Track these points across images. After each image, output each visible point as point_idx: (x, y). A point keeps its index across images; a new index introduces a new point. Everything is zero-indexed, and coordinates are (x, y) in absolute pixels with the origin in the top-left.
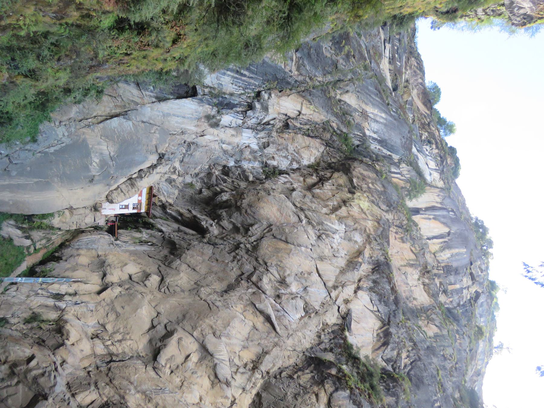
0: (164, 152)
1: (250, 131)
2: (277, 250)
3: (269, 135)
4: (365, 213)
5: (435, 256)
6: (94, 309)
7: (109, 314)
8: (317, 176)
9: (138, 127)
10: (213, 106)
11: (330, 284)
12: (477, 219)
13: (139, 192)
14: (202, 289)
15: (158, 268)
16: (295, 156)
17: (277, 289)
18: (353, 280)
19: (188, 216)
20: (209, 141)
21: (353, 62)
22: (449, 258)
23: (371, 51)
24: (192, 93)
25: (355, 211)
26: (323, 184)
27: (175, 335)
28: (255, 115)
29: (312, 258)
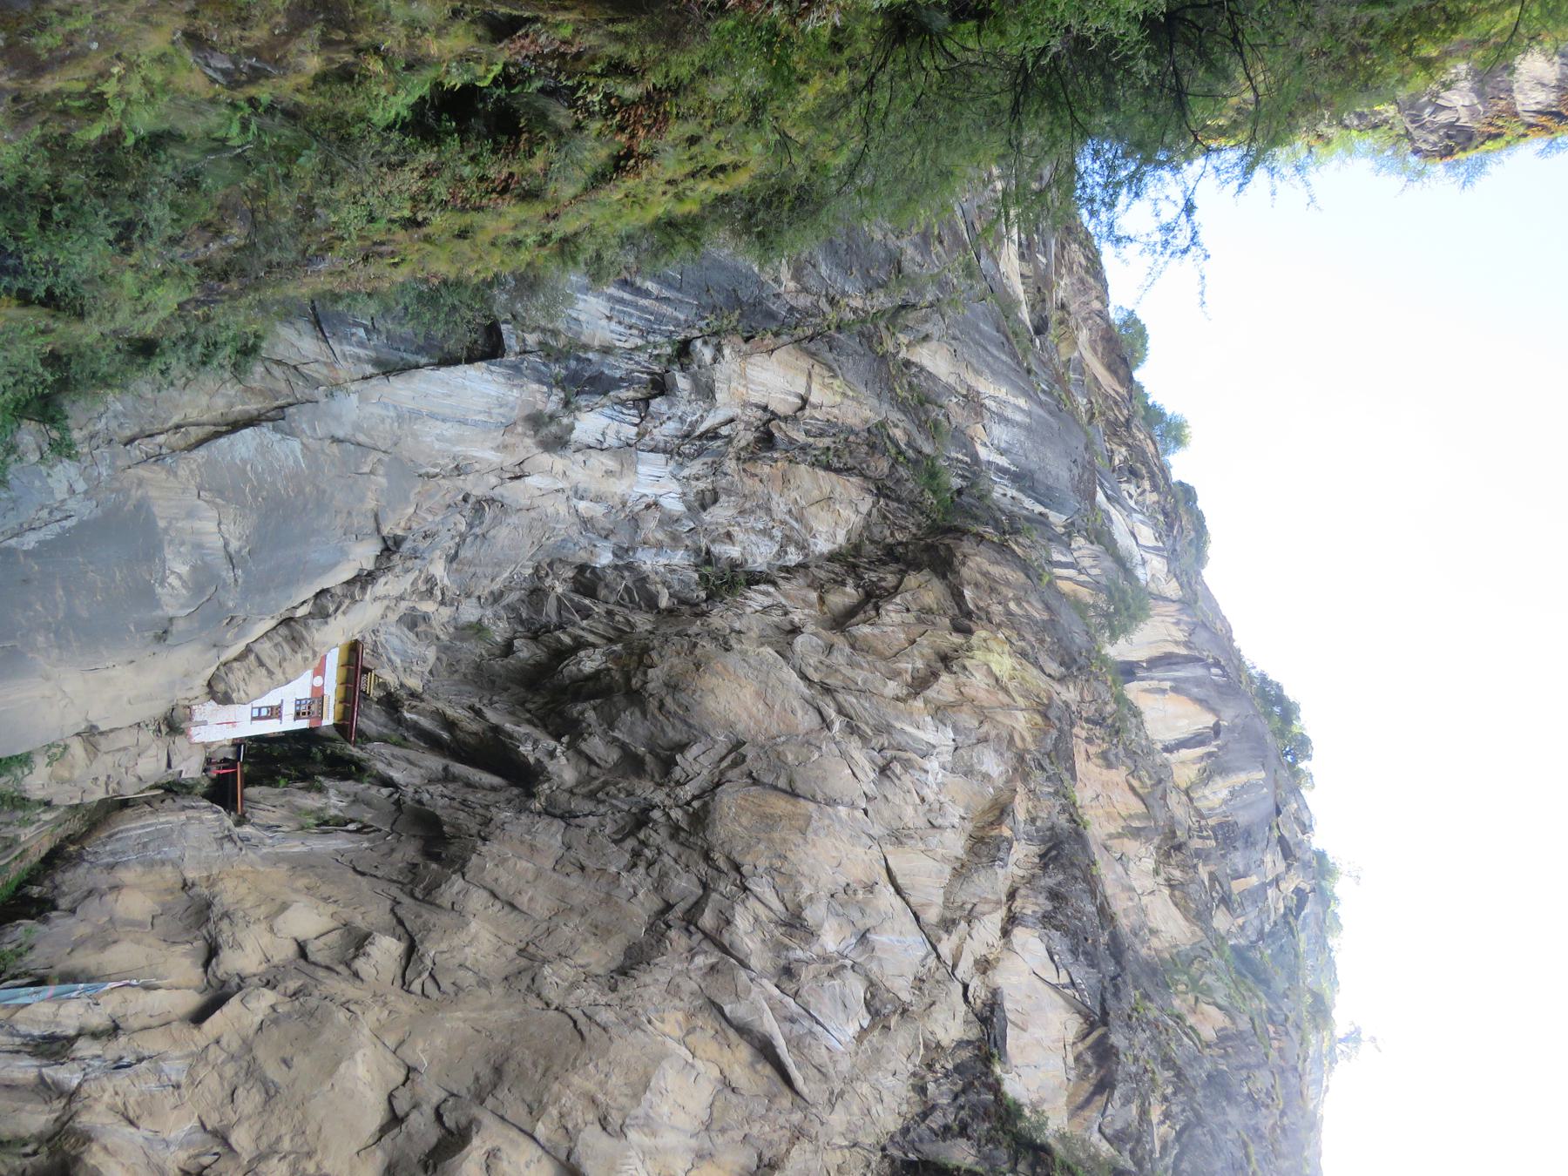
0: (400, 532)
1: (661, 458)
2: (768, 822)
3: (716, 469)
4: (1006, 691)
5: (1191, 800)
6: (183, 1080)
7: (240, 1091)
8: (857, 586)
9: (322, 458)
10: (550, 386)
11: (932, 915)
12: (1263, 678)
13: (317, 662)
14: (547, 970)
15: (392, 910)
16: (792, 528)
17: (779, 948)
18: (994, 898)
19: (475, 727)
20: (538, 493)
21: (938, 257)
22: (1225, 802)
23: (977, 225)
24: (488, 348)
25: (978, 684)
26: (877, 609)
27: (476, 1141)
29: (870, 836)
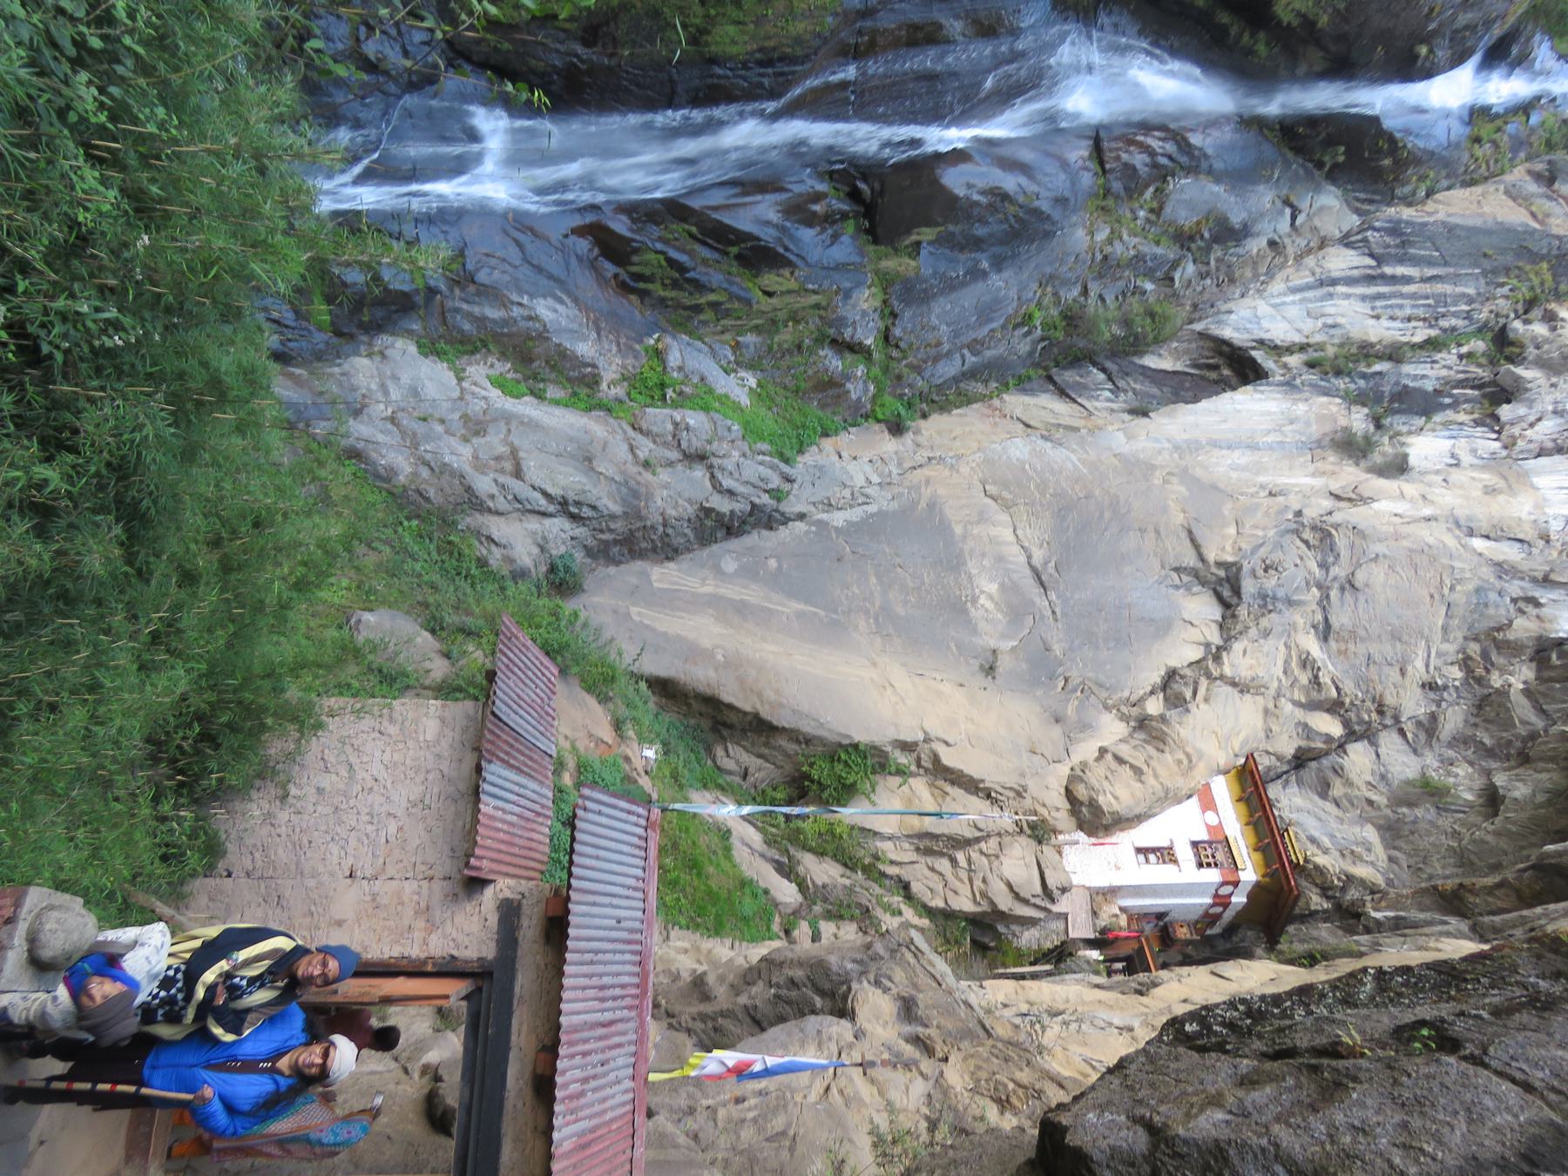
0: (1230, 559)
28: (1538, 407)
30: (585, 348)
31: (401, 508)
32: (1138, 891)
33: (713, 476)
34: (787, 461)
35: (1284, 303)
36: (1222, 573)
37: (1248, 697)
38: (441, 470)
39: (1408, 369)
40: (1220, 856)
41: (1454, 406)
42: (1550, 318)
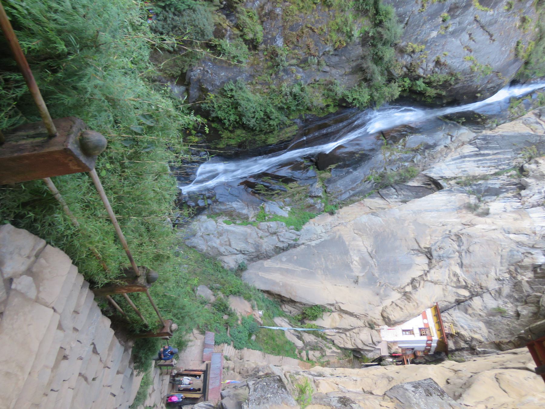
0: (428, 246)
28: (533, 191)
30: (245, 211)
31: (205, 257)
32: (403, 342)
33: (278, 238)
34: (298, 230)
35: (450, 164)
36: (426, 250)
37: (437, 285)
38: (213, 247)
39: (490, 182)
40: (427, 332)
41: (507, 191)
42: (537, 163)
